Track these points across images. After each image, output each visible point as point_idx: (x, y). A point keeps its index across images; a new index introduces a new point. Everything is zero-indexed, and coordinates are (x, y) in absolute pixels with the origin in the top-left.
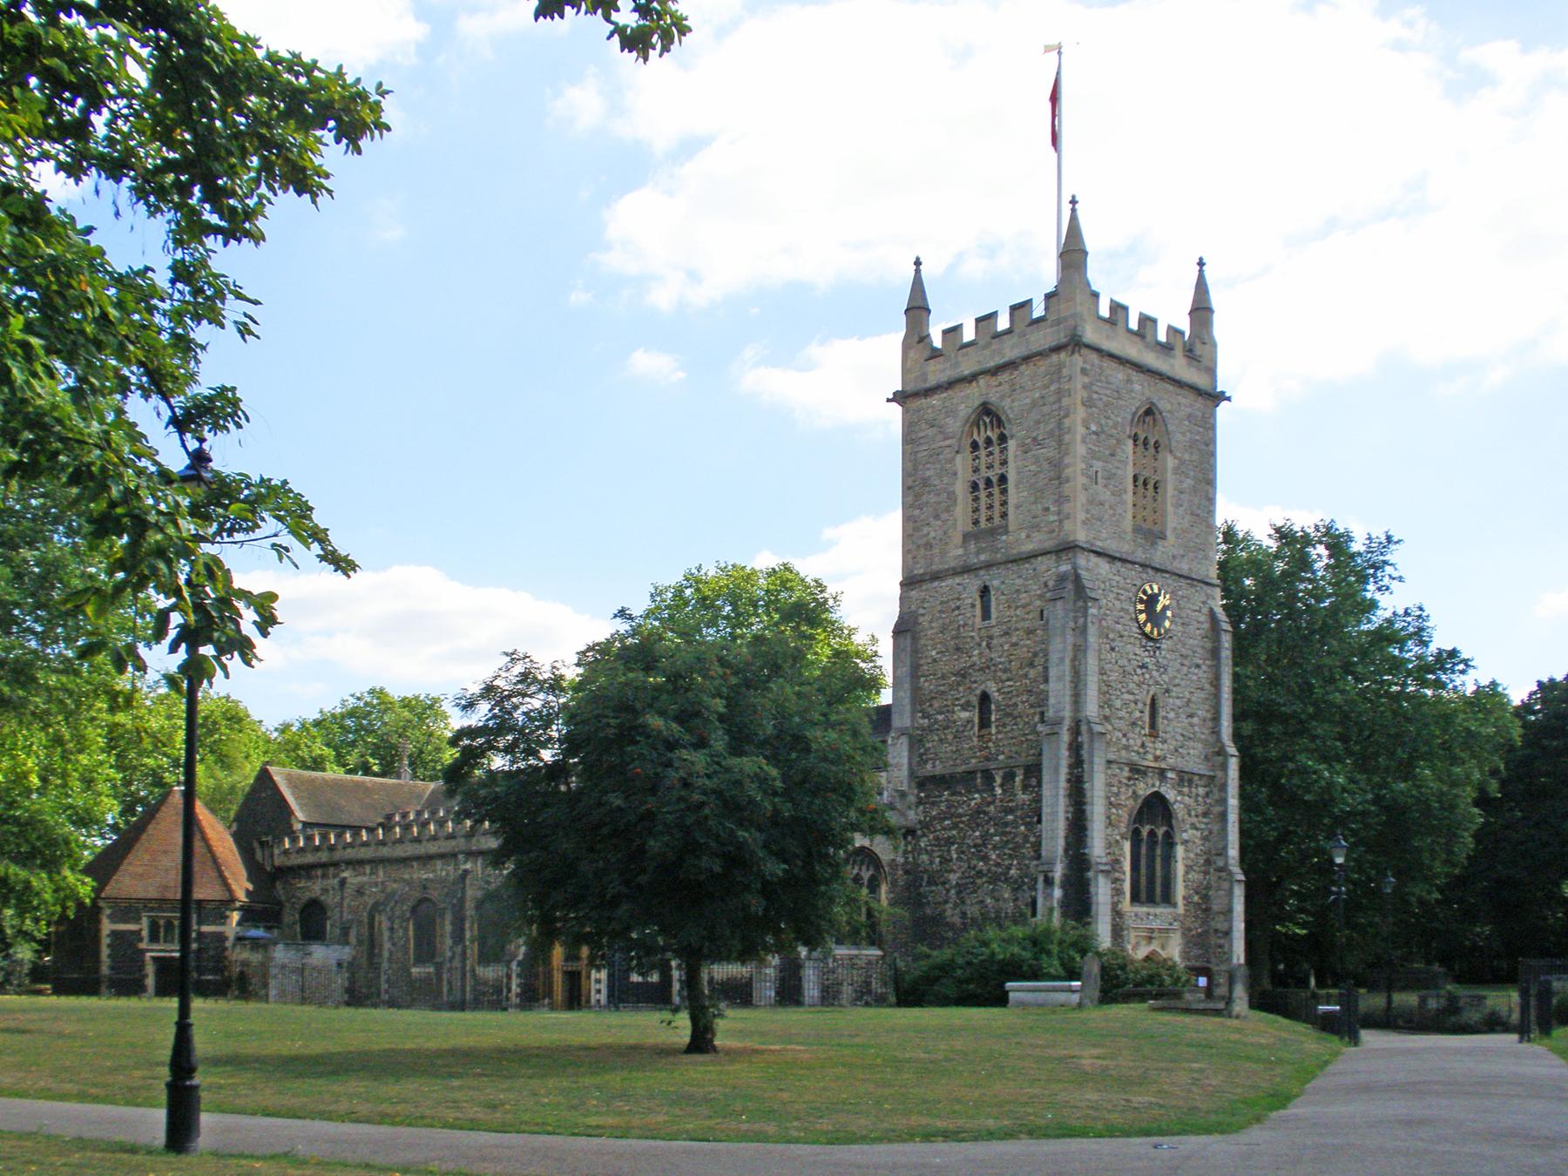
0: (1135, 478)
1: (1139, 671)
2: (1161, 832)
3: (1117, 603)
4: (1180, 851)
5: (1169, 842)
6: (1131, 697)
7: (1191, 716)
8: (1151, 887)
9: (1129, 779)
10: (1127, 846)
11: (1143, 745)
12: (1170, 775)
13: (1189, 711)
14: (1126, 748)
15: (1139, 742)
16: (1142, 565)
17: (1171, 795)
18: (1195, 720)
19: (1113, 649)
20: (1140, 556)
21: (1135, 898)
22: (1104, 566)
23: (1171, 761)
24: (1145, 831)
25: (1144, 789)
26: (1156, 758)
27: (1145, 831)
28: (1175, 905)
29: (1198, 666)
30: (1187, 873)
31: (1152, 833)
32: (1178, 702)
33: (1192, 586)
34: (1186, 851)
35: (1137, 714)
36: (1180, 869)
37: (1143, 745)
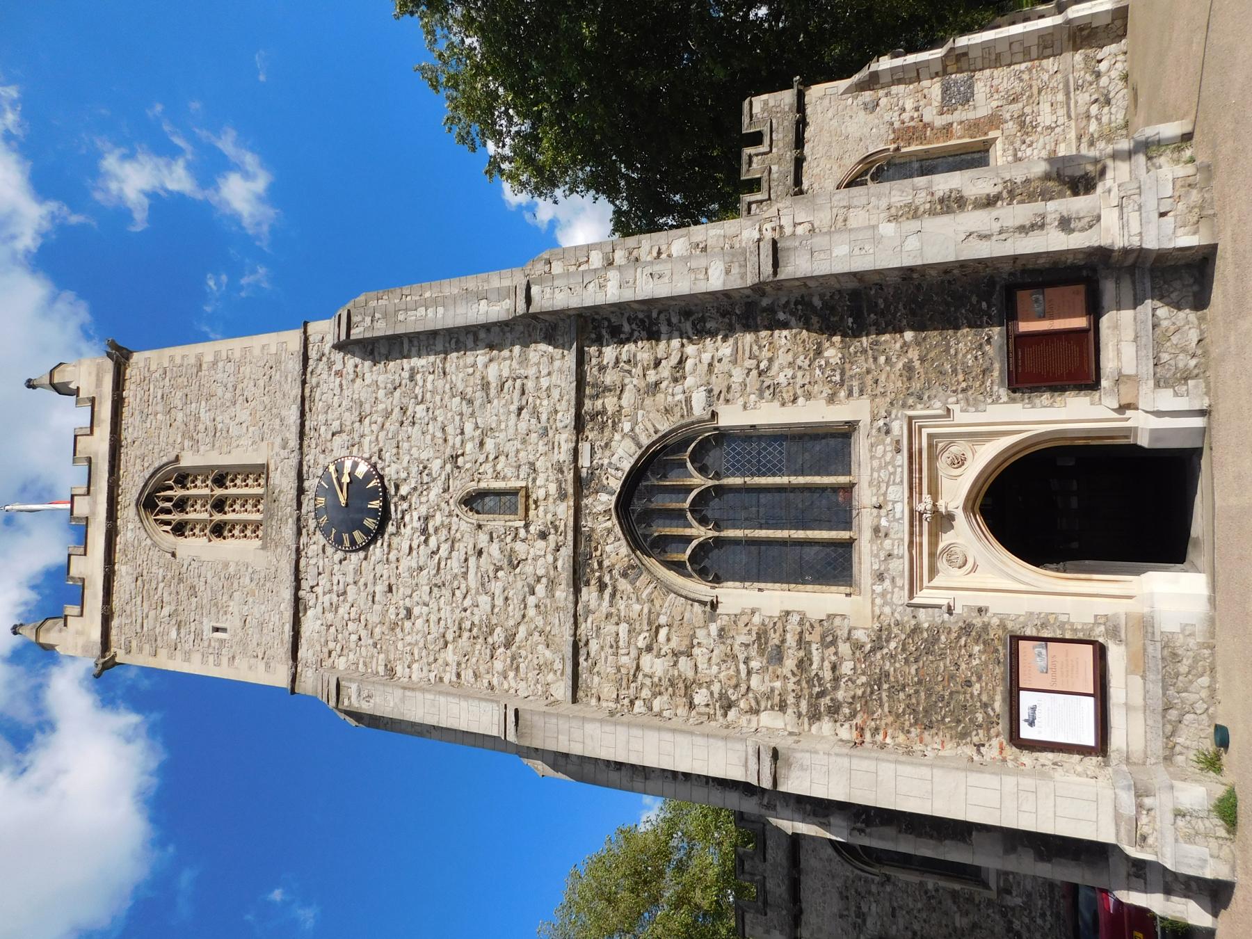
0: (218, 530)
1: (433, 541)
3: (351, 590)
4: (730, 417)
7: (486, 386)
9: (602, 587)
11: (543, 536)
15: (541, 544)
16: (299, 533)
19: (409, 612)
20: (289, 530)
22: (310, 624)
25: (616, 550)
26: (562, 496)
27: (700, 533)
28: (852, 426)
29: (412, 378)
32: (469, 427)
34: (726, 394)
35: (495, 549)
36: (769, 414)
37: (543, 536)
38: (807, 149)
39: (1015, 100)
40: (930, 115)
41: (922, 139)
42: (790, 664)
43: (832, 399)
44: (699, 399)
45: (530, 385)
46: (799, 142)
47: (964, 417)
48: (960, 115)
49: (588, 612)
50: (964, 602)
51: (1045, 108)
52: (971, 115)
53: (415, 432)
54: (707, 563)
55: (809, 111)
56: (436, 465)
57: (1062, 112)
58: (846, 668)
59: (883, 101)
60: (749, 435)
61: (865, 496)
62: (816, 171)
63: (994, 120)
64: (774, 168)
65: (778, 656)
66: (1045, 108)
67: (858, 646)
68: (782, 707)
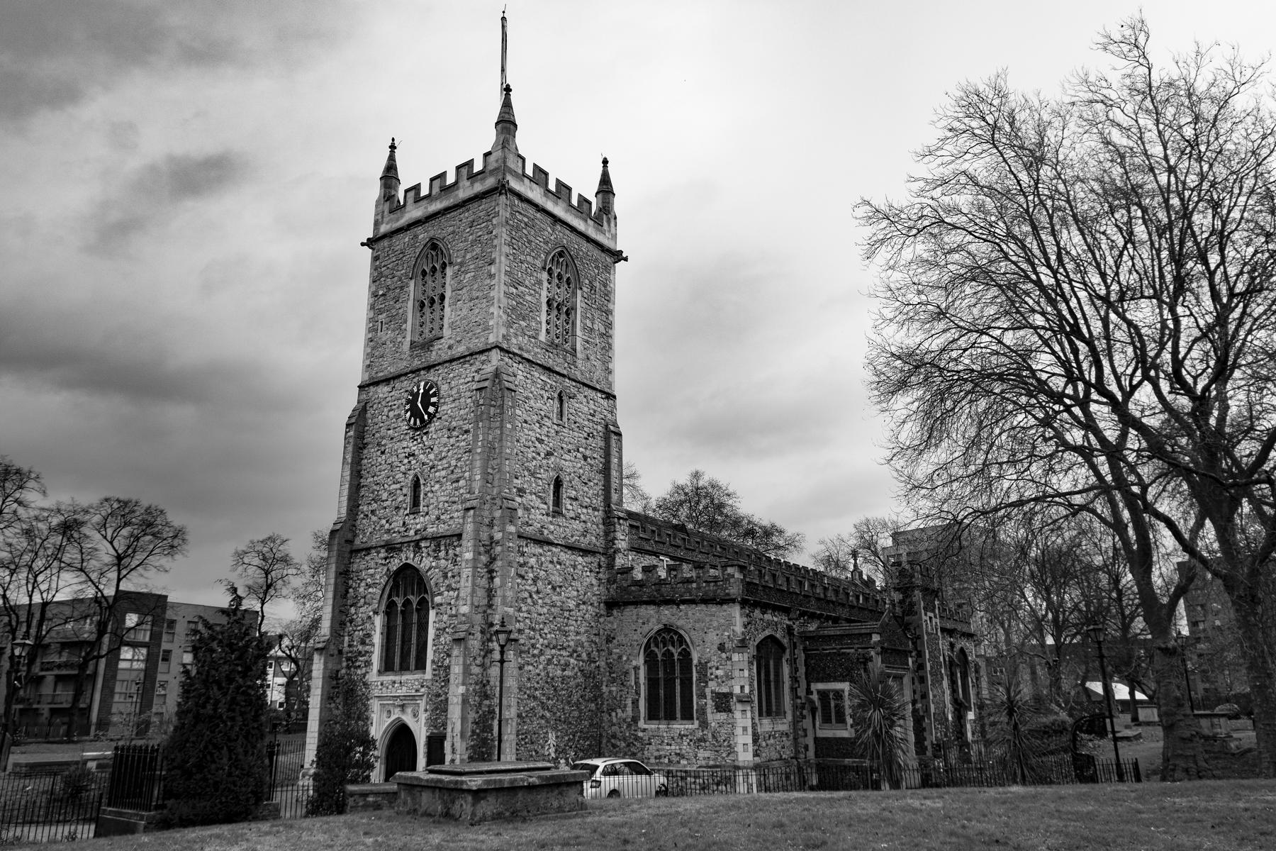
1: (406, 461)
2: (414, 599)
5: (424, 606)
6: (398, 486)
8: (405, 652)
9: (386, 559)
10: (378, 621)
12: (423, 544)
13: (454, 477)
14: (388, 531)
17: (425, 563)
18: (462, 483)
21: (387, 667)
23: (431, 530)
24: (399, 601)
25: (395, 564)
27: (399, 601)
30: (438, 636)
31: (407, 603)
32: (443, 473)
33: (464, 363)
35: (401, 498)
38: (703, 607)
39: (714, 736)
40: (712, 685)
41: (699, 680)
42: (360, 648)
43: (433, 662)
44: (438, 599)
45: (455, 507)
46: (705, 601)
47: (423, 716)
48: (710, 703)
49: (378, 553)
50: (374, 717)
51: (707, 754)
52: (709, 710)
53: (445, 440)
54: (390, 610)
55: (725, 607)
56: (432, 456)
57: (704, 763)
58: (359, 672)
59: (724, 655)
60: (423, 627)
61: (406, 677)
62: (690, 613)
63: (704, 724)
64: (694, 585)
65: (363, 643)
66: (707, 754)
67: (364, 675)
68: (350, 646)
